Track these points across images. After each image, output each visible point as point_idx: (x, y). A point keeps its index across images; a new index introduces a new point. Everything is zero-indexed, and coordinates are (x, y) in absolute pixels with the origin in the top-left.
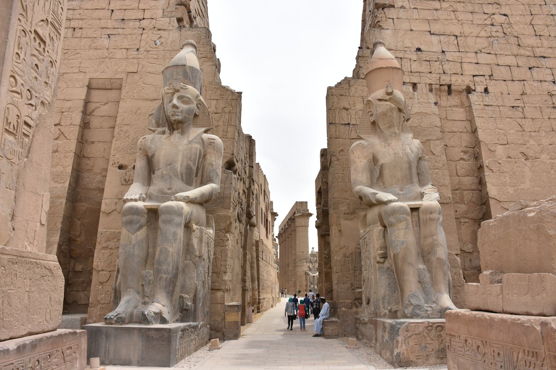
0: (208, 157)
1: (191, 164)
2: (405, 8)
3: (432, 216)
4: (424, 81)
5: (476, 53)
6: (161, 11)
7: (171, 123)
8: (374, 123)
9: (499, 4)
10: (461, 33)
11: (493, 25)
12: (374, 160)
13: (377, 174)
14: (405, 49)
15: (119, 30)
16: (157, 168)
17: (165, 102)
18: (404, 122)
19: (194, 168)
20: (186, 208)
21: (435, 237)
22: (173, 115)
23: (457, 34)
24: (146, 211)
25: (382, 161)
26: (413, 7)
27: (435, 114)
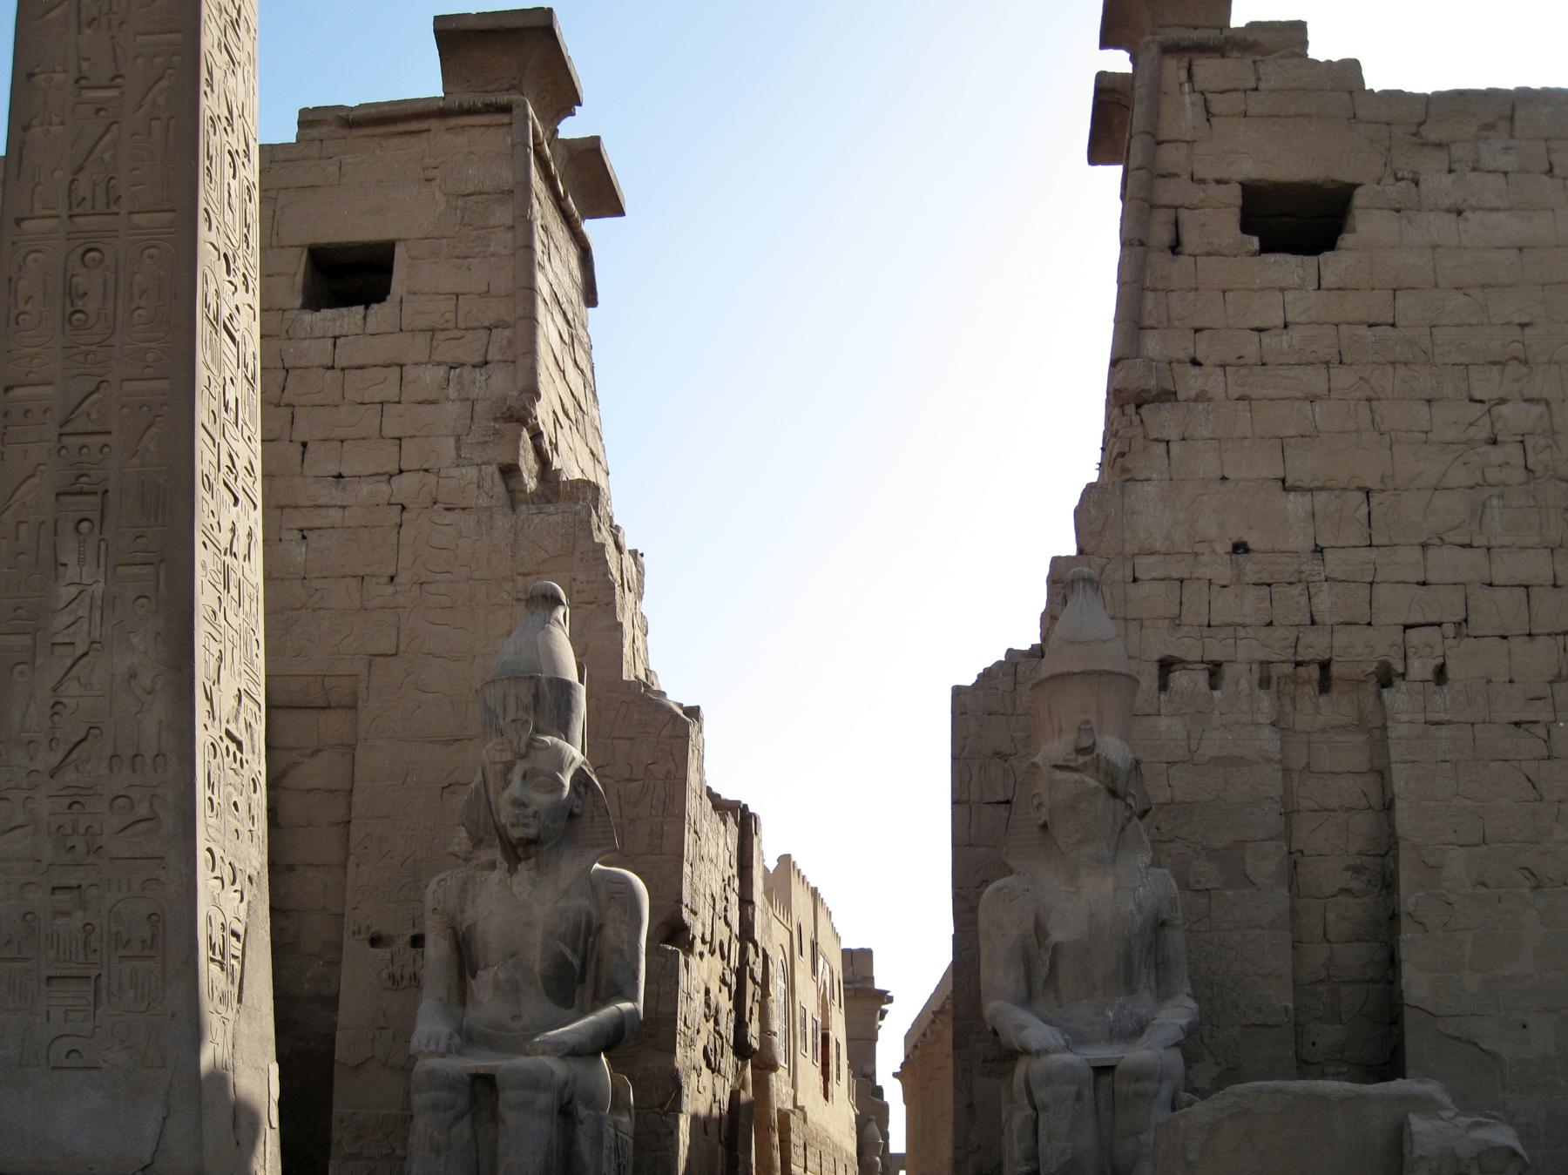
0: (609, 932)
1: (568, 952)
2: (1210, 400)
3: (1140, 1087)
4: (1243, 654)
5: (1424, 546)
6: (452, 441)
7: (510, 842)
8: (1044, 826)
9: (1525, 363)
10: (1382, 480)
11: (1494, 442)
12: (1040, 929)
13: (1043, 971)
14: (1199, 548)
15: (332, 512)
16: (482, 964)
17: (491, 787)
18: (1129, 820)
19: (576, 962)
20: (558, 1068)
21: (1142, 1138)
22: (513, 825)
23: (1369, 485)
24: (468, 1079)
25: (1057, 936)
26: (1236, 392)
27: (1269, 760)
